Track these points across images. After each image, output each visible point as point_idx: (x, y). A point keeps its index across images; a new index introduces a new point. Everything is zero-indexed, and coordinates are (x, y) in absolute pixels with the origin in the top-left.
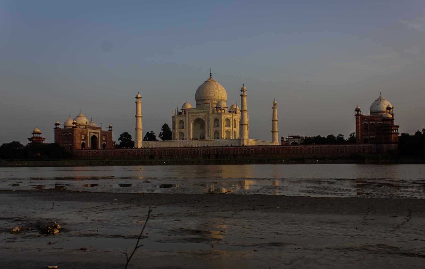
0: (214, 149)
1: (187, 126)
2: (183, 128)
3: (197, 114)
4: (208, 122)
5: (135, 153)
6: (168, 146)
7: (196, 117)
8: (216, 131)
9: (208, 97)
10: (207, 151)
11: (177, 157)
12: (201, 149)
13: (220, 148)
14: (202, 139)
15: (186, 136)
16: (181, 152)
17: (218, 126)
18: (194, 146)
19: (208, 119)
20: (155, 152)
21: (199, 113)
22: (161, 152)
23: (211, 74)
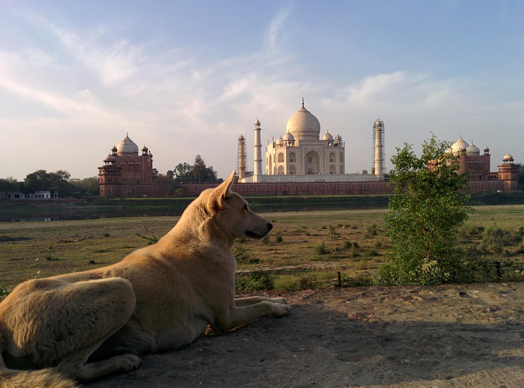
2: (291, 161)
4: (324, 156)
5: (264, 189)
6: (297, 181)
7: (310, 150)
10: (350, 187)
11: (315, 192)
12: (342, 185)
15: (298, 171)
16: (320, 187)
17: (331, 161)
19: (324, 152)
20: (289, 188)
21: (314, 145)
23: (303, 104)
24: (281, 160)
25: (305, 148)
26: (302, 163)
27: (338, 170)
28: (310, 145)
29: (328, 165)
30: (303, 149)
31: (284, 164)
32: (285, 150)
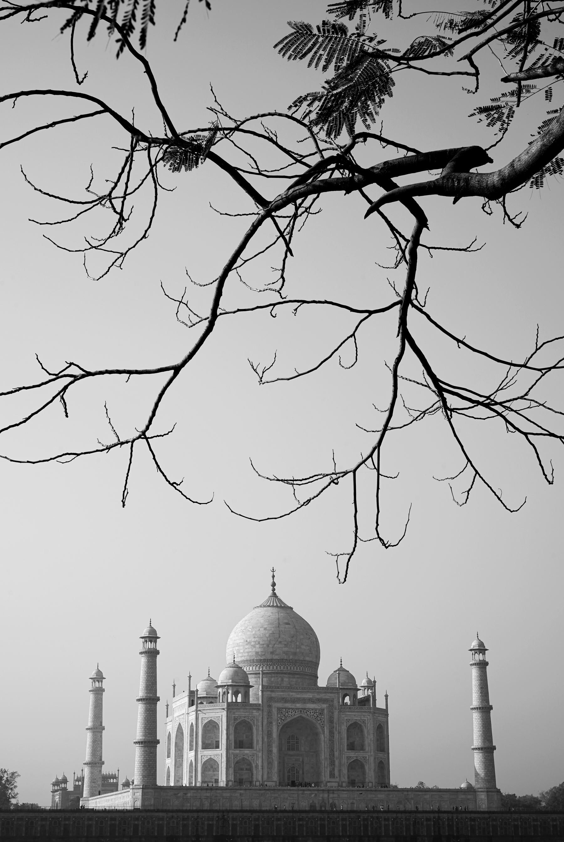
0: (428, 820)
1: (266, 740)
3: (298, 705)
8: (356, 761)
9: (295, 654)
13: (445, 815)
14: (293, 784)
17: (351, 747)
18: (342, 807)
19: (331, 721)
21: (304, 701)
22: (257, 826)
23: (274, 585)
24: (210, 743)
25: (279, 709)
26: (270, 752)
27: (371, 775)
28: (294, 701)
29: (344, 760)
30: (275, 711)
31: (220, 755)
32: (224, 713)
